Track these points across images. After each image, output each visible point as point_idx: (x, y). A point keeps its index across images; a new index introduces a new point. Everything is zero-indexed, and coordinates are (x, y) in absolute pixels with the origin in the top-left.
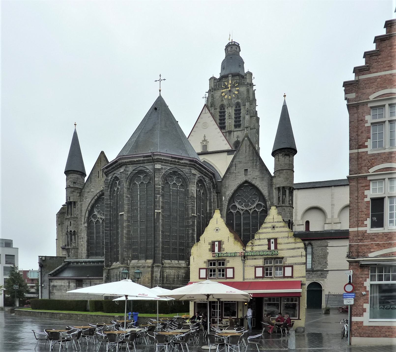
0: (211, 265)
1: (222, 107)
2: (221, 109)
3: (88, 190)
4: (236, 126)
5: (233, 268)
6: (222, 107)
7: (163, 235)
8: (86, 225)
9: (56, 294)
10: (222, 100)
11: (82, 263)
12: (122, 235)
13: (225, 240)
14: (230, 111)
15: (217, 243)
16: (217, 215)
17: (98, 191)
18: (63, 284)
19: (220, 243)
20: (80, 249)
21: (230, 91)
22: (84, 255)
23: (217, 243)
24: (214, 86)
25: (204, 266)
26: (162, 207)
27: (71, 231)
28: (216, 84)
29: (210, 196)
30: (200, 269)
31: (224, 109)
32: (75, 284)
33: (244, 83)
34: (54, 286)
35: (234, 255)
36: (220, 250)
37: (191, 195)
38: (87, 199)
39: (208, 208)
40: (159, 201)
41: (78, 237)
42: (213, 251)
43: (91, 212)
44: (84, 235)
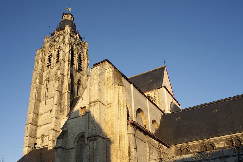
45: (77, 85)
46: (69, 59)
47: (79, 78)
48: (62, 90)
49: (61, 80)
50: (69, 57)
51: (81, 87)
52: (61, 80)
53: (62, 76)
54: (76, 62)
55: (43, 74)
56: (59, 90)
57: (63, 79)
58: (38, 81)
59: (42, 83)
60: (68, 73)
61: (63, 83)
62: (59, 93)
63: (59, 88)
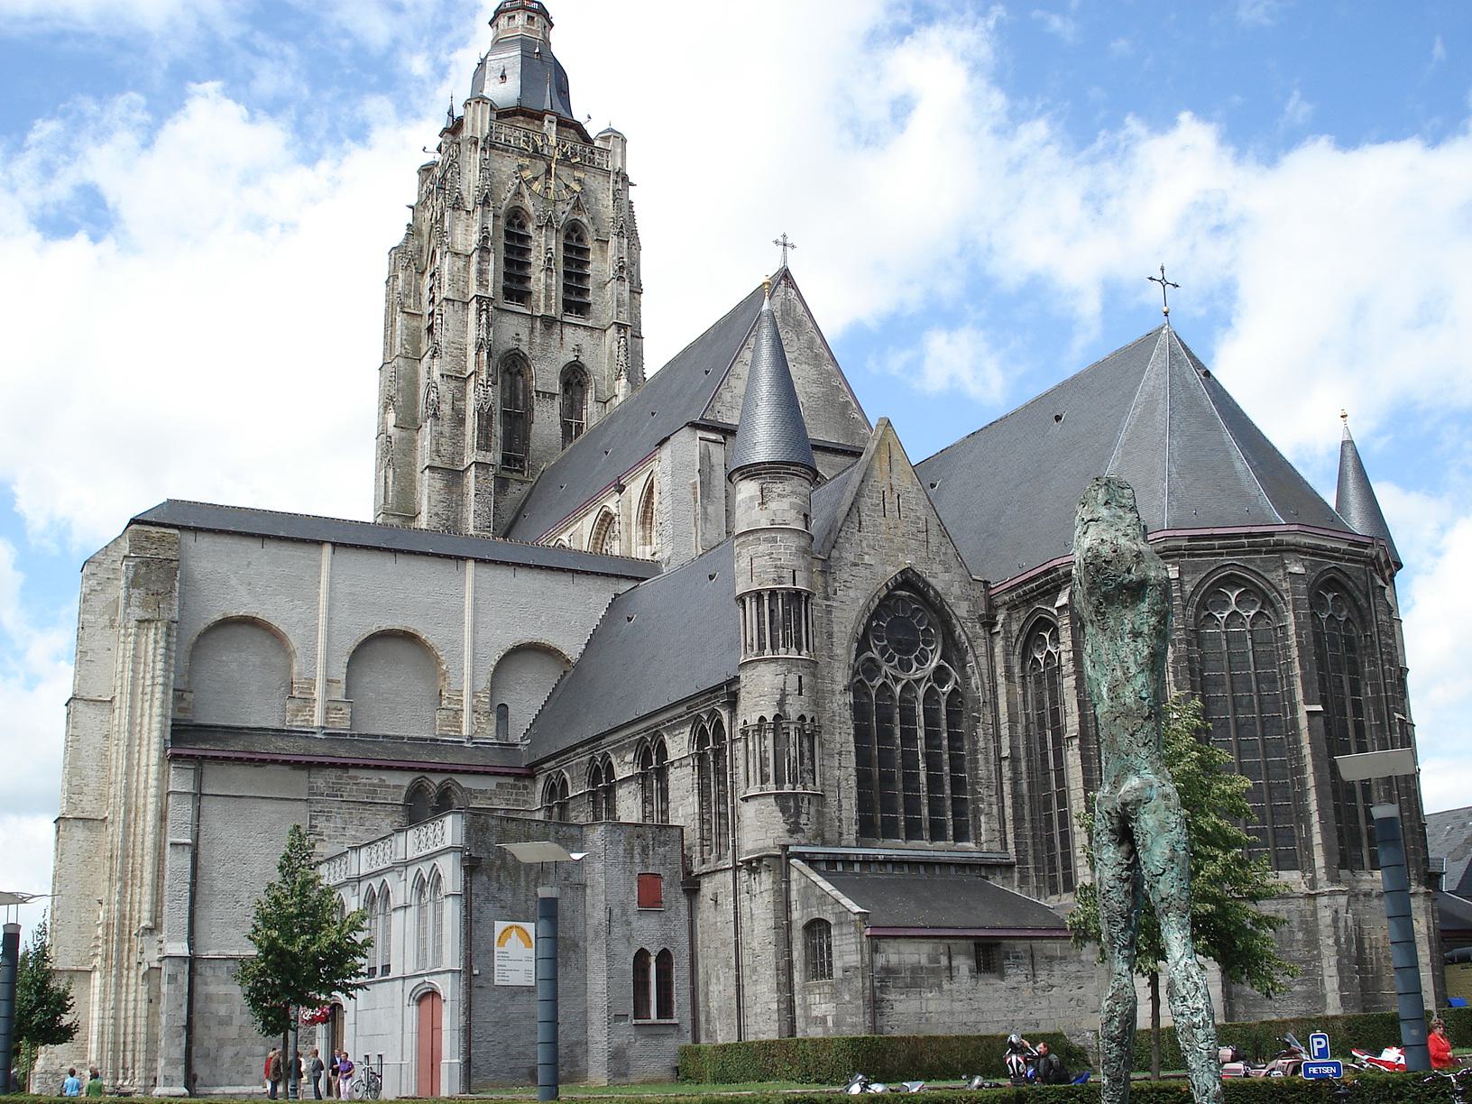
2: (509, 223)
3: (851, 557)
8: (850, 698)
9: (899, 1007)
11: (852, 863)
12: (987, 760)
17: (892, 571)
18: (924, 961)
20: (831, 800)
22: (851, 831)
27: (802, 718)
31: (522, 226)
32: (972, 963)
34: (889, 971)
38: (852, 593)
41: (822, 745)
43: (863, 644)
44: (842, 738)
45: (558, 400)
46: (481, 284)
48: (458, 453)
49: (446, 409)
50: (481, 272)
51: (590, 395)
52: (446, 409)
53: (453, 384)
54: (544, 283)
55: (416, 372)
56: (438, 463)
57: (459, 397)
58: (391, 418)
59: (415, 419)
60: (477, 363)
61: (460, 420)
62: (437, 476)
63: (438, 451)
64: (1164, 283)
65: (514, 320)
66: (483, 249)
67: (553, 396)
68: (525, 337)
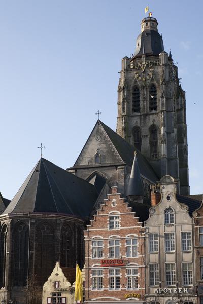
0: (54, 296)
1: (136, 88)
4: (151, 109)
5: (65, 298)
6: (137, 88)
7: (35, 269)
10: (136, 81)
13: (61, 280)
14: (144, 94)
15: (57, 282)
16: (58, 264)
19: (59, 282)
21: (144, 72)
23: (57, 282)
24: (127, 68)
25: (51, 296)
26: (35, 249)
28: (130, 64)
29: (75, 234)
30: (48, 298)
33: (159, 63)
35: (65, 291)
36: (58, 287)
37: (56, 238)
39: (73, 244)
40: (33, 245)
42: (55, 287)
47: (152, 124)
64: (41, 148)
65: (136, 118)
66: (124, 102)
67: (147, 136)
68: (139, 122)
